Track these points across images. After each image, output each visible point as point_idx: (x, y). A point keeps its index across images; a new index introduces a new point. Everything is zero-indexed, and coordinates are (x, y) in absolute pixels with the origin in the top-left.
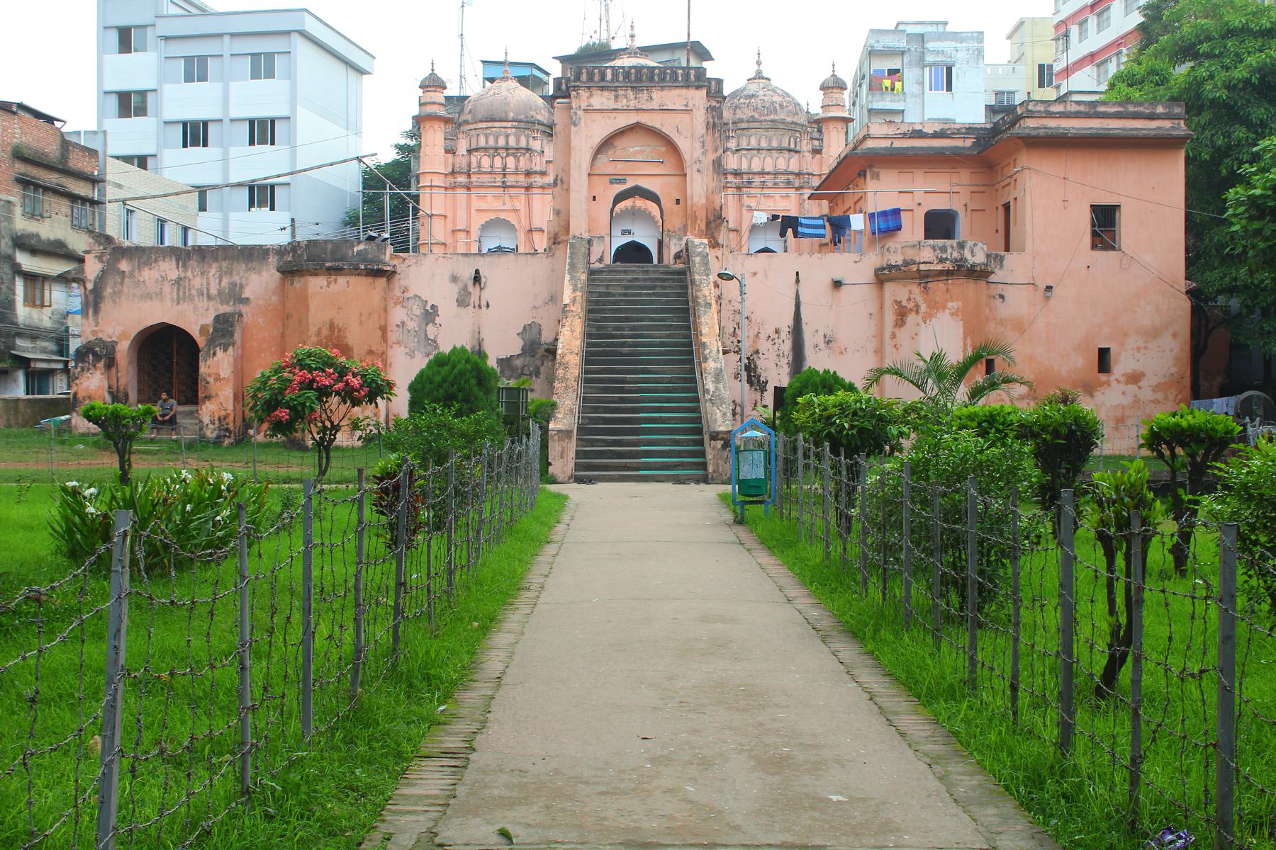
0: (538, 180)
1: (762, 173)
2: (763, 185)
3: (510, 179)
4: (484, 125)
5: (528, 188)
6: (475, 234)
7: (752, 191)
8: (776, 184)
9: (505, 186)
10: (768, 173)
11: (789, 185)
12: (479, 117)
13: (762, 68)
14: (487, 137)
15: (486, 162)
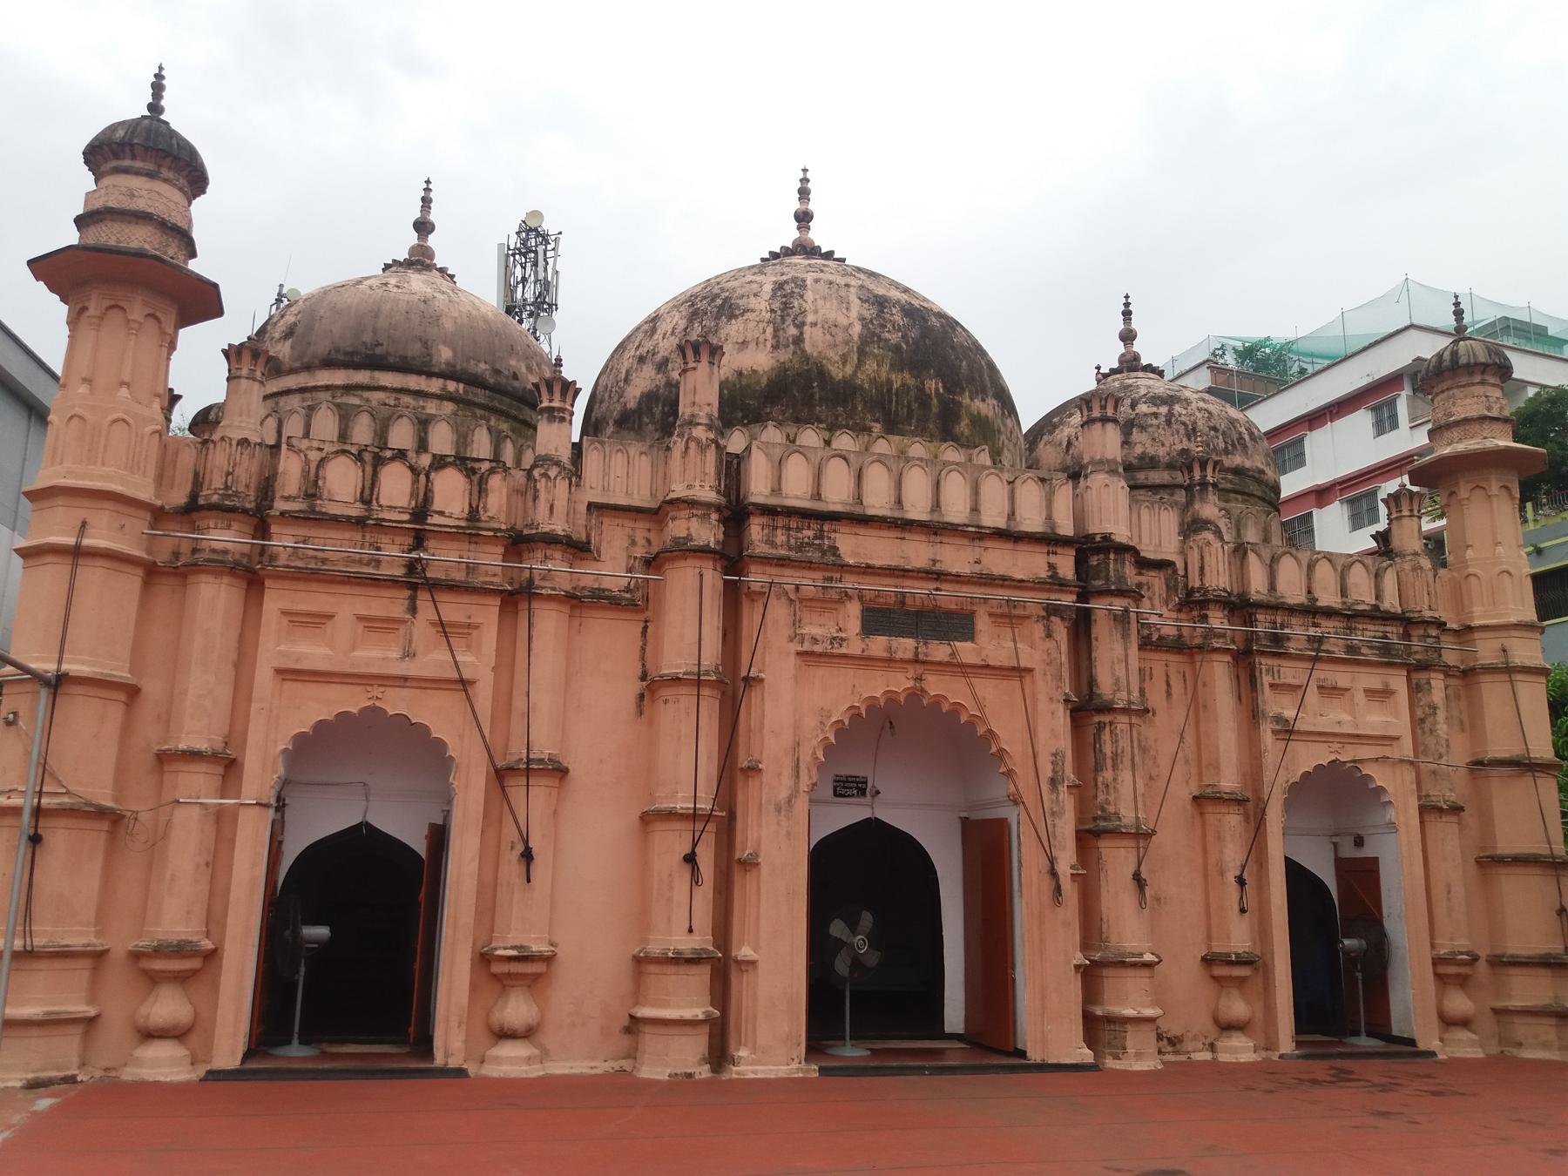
0: (555, 570)
1: (1311, 611)
2: (1317, 654)
3: (444, 558)
4: (339, 377)
5: (516, 598)
6: (259, 778)
7: (1291, 673)
8: (1351, 649)
9: (416, 581)
10: (1329, 613)
11: (1388, 657)
12: (321, 348)
13: (1137, 346)
14: (346, 417)
15: (342, 481)
